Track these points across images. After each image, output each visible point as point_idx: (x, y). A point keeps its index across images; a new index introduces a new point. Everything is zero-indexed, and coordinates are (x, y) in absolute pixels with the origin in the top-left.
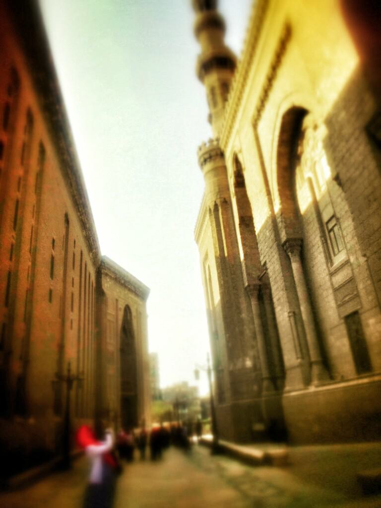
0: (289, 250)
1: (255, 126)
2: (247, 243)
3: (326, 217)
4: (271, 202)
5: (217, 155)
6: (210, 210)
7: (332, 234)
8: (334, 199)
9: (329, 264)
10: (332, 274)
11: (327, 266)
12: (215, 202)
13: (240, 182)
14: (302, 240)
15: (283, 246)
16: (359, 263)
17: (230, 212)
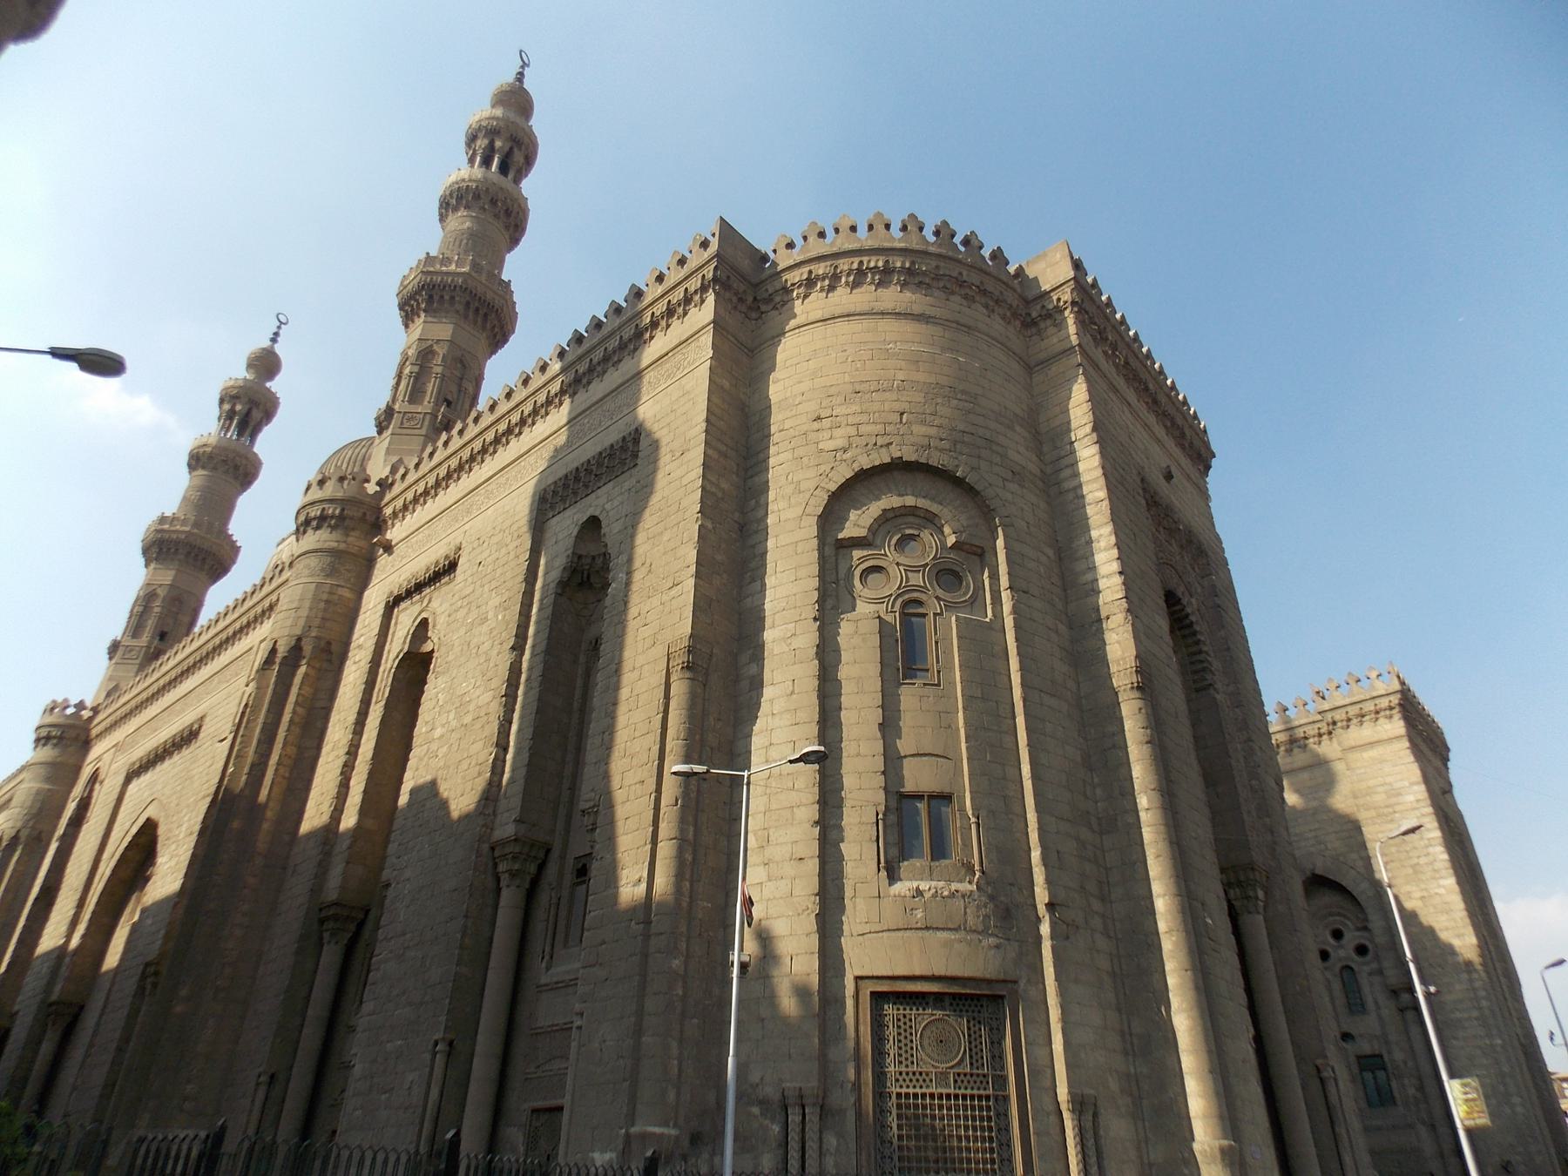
5: (363, 518)
6: (273, 651)
12: (299, 639)
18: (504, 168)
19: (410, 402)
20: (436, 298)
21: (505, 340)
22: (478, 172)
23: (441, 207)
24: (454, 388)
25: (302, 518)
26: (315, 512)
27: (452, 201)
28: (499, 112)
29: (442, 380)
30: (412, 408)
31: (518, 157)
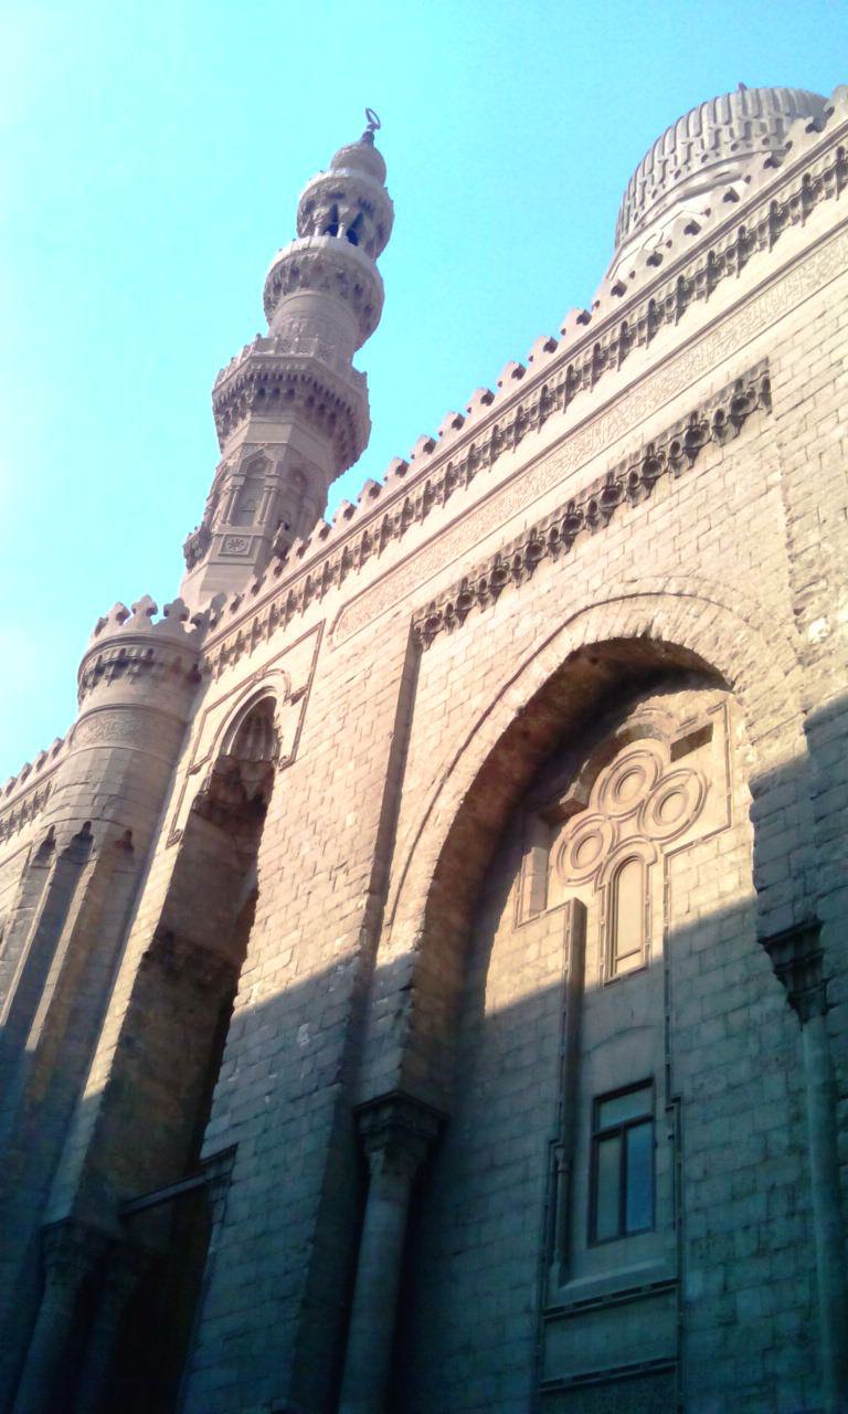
0: (386, 1138)
1: (420, 637)
2: (139, 1044)
3: (602, 1073)
4: (373, 926)
5: (176, 668)
7: (610, 1150)
8: (690, 1015)
9: (556, 1268)
10: (552, 1316)
11: (543, 1276)
12: (87, 825)
13: (237, 803)
14: (444, 1123)
15: (359, 1112)
16: (734, 1311)
17: (125, 892)
18: (352, 236)
19: (235, 521)
20: (268, 391)
21: (356, 459)
22: (319, 240)
23: (268, 290)
24: (293, 510)
25: (92, 664)
26: (111, 654)
27: (286, 278)
28: (344, 172)
29: (278, 494)
30: (239, 530)
31: (369, 226)
